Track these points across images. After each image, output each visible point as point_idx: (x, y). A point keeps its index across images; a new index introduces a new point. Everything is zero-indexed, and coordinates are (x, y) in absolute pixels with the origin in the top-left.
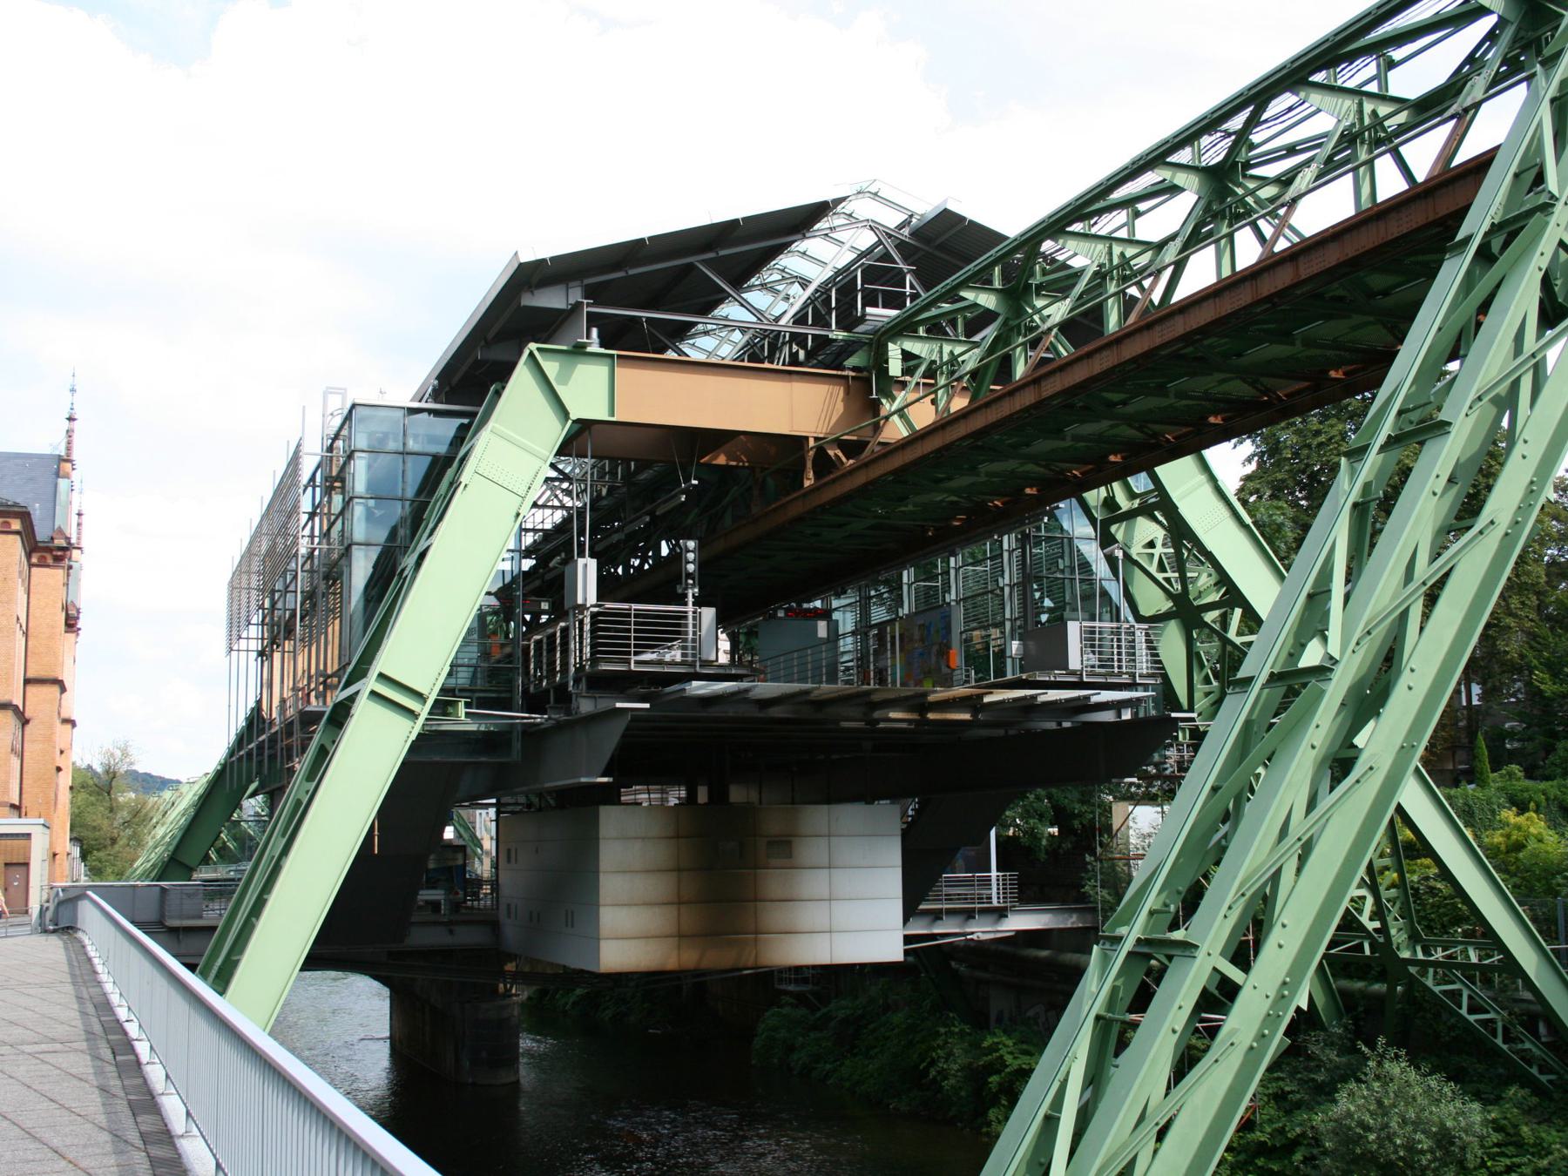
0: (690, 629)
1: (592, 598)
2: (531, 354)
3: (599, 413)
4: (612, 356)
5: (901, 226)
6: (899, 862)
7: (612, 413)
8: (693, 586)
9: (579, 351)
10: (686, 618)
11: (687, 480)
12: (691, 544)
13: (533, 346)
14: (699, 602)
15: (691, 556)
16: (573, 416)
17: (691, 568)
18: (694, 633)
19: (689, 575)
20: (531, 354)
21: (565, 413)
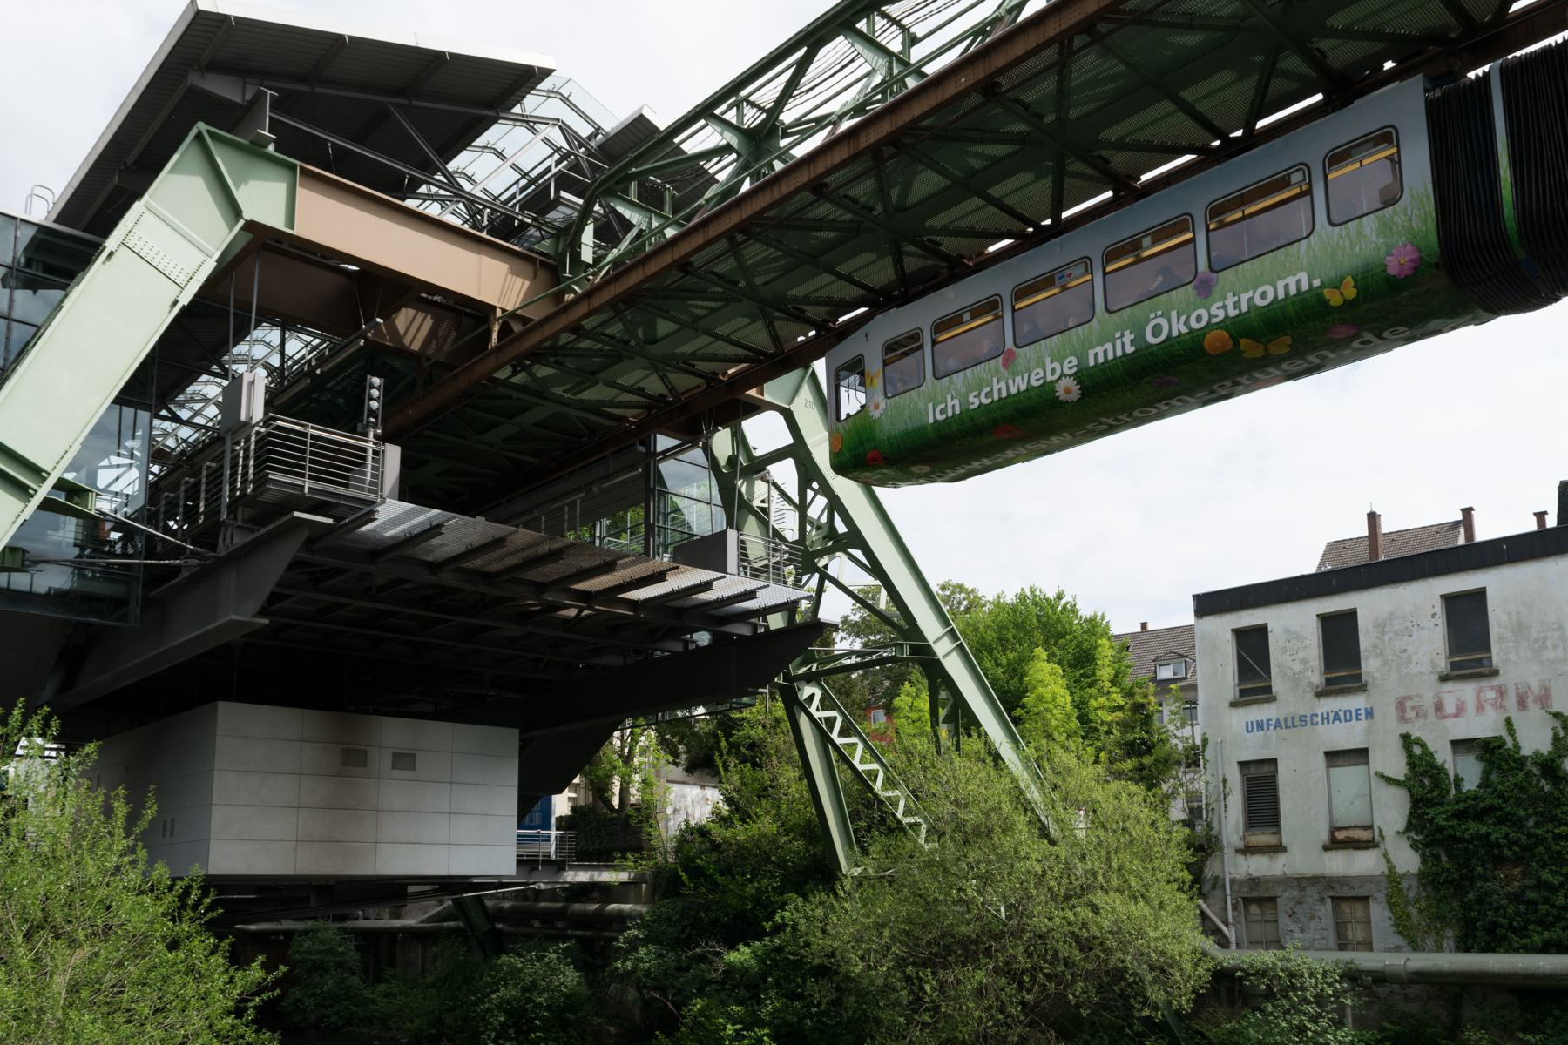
0: (369, 470)
1: (258, 413)
2: (199, 136)
3: (277, 221)
4: (292, 168)
5: (590, 137)
6: (516, 783)
7: (291, 221)
8: (375, 425)
9: (255, 150)
10: (364, 458)
11: (370, 319)
12: (376, 381)
13: (201, 126)
14: (386, 438)
15: (375, 393)
16: (249, 214)
17: (374, 405)
18: (373, 476)
19: (372, 413)
20: (199, 136)
21: (234, 210)
